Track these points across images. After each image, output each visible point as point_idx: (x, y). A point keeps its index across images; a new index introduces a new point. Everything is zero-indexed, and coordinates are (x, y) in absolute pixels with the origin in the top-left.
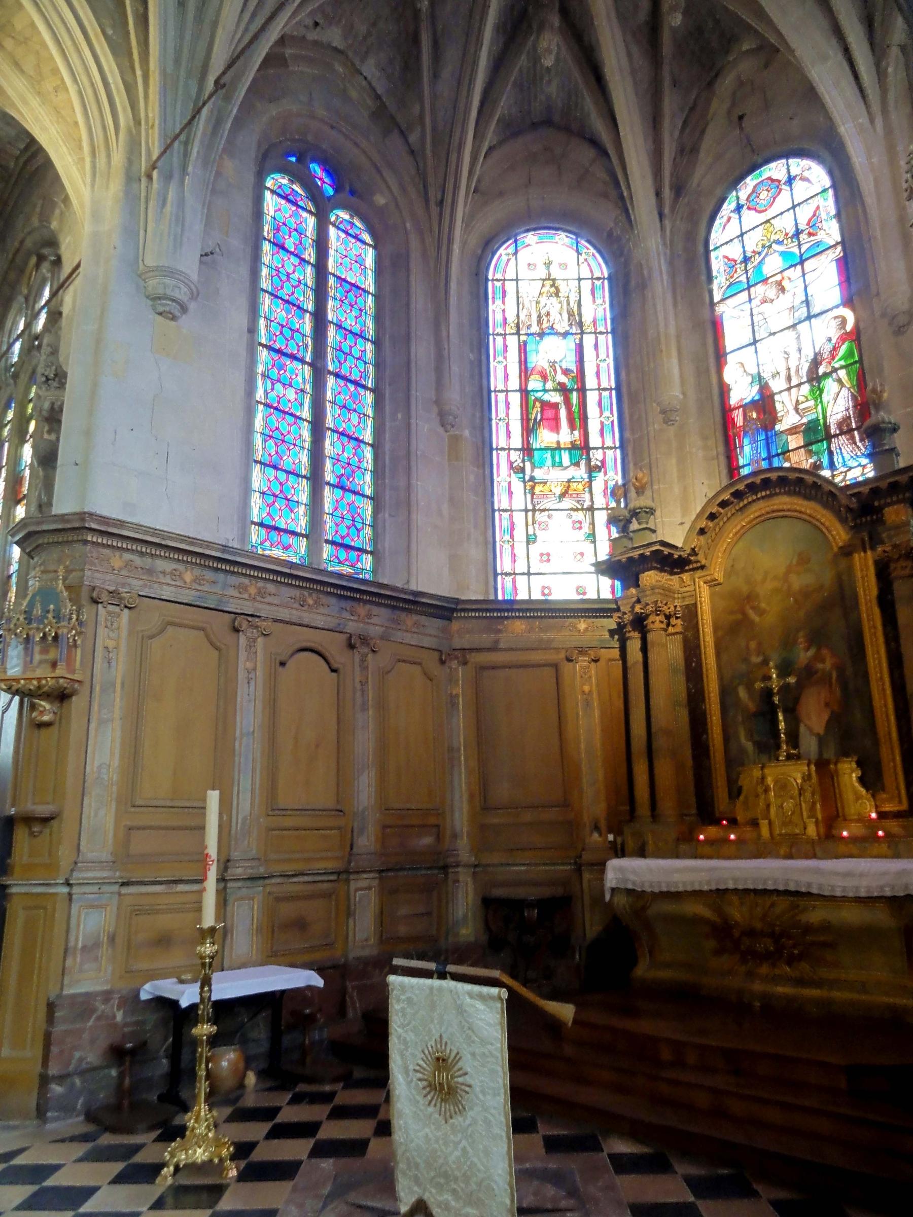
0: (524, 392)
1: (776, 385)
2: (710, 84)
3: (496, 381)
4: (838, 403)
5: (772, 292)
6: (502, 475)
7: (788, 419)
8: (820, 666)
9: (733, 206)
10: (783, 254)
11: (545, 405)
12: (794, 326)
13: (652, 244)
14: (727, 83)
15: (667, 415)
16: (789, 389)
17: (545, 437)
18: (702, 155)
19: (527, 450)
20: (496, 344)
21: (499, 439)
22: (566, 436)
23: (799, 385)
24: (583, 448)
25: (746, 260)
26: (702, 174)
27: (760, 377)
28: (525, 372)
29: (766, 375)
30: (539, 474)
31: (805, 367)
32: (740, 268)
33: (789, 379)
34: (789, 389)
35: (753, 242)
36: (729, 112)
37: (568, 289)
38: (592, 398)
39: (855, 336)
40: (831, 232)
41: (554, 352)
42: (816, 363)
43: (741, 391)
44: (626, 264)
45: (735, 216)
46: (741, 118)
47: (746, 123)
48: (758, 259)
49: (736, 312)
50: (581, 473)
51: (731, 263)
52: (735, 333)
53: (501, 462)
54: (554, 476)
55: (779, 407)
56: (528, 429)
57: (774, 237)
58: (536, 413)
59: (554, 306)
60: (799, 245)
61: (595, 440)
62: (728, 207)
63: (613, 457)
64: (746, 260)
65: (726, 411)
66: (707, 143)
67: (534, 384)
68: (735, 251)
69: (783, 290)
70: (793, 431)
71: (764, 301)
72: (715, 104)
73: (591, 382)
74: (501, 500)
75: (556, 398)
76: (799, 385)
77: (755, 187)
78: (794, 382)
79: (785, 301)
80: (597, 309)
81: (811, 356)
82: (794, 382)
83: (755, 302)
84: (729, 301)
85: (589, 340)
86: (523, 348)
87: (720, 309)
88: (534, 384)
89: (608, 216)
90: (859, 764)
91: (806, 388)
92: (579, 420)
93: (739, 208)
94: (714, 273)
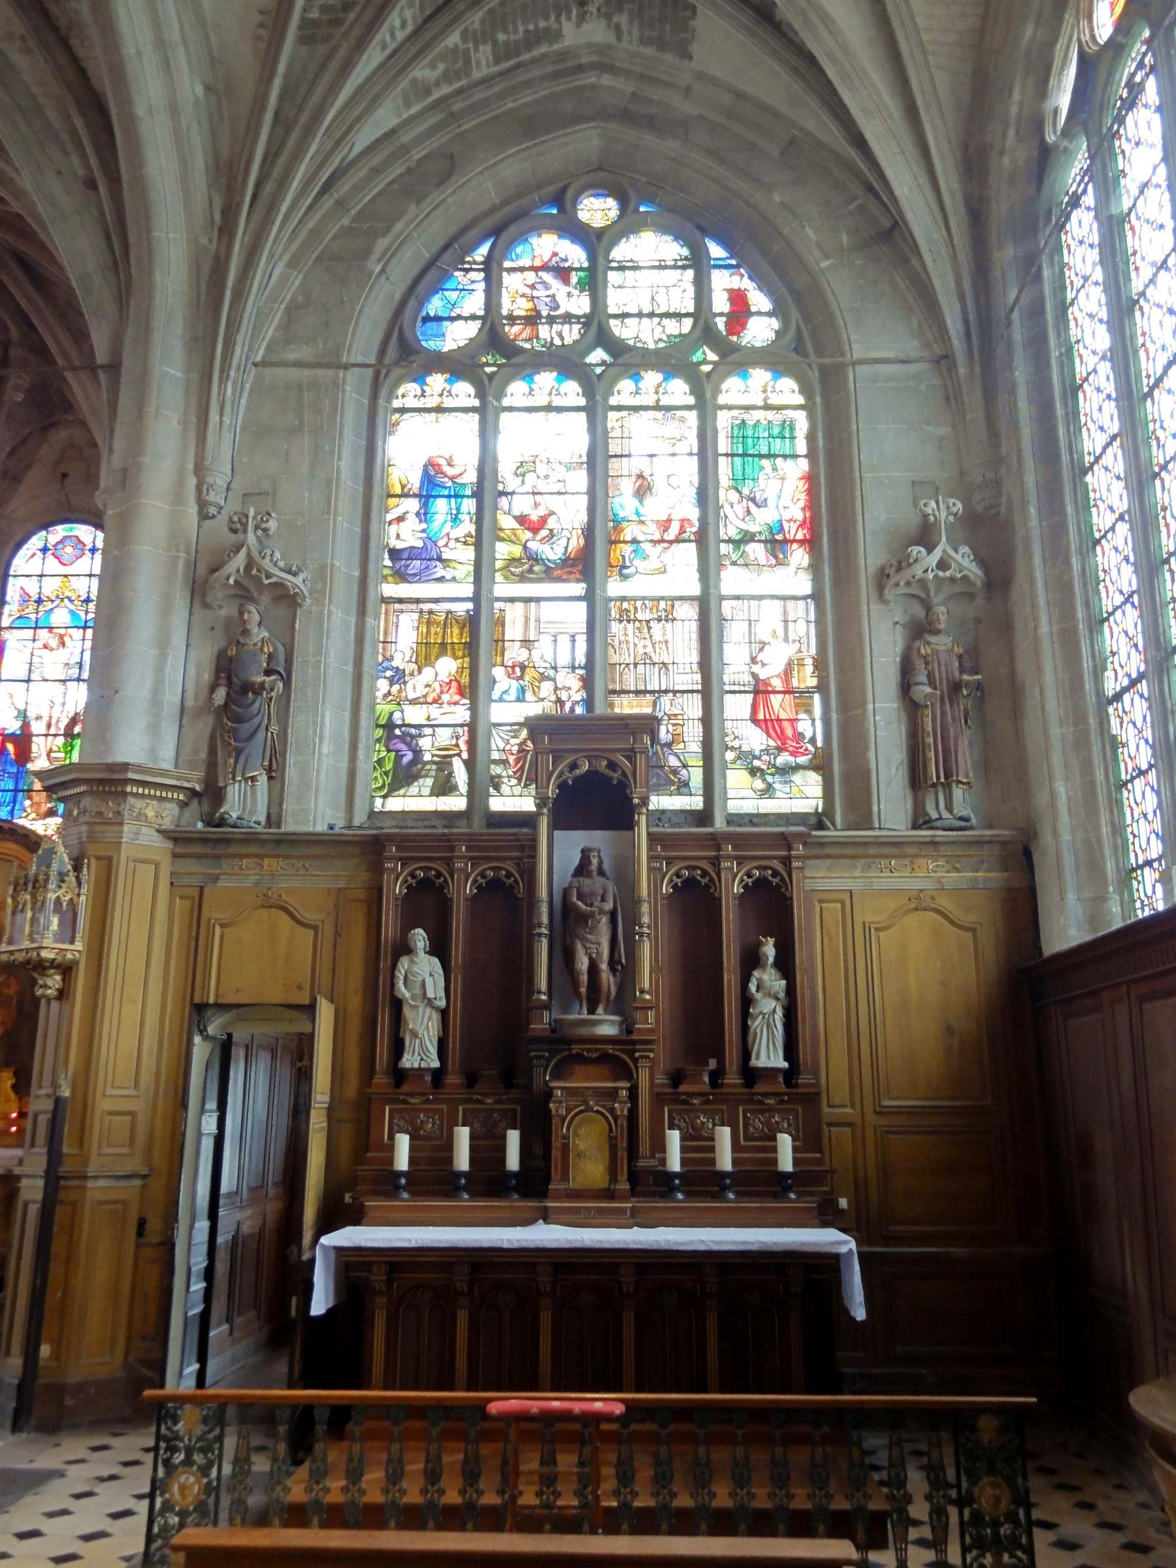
1: (37, 728)
2: (45, 429)
5: (54, 643)
7: (40, 763)
8: (6, 991)
9: (41, 545)
10: (71, 612)
12: (64, 681)
16: (46, 735)
18: (22, 488)
23: (55, 735)
25: (39, 601)
27: (25, 716)
29: (31, 714)
31: (64, 722)
32: (32, 607)
33: (49, 726)
34: (46, 735)
35: (50, 587)
36: (57, 463)
42: (74, 721)
45: (40, 554)
46: (64, 475)
47: (67, 481)
48: (49, 605)
49: (19, 645)
51: (25, 598)
55: (34, 748)
57: (67, 593)
60: (87, 612)
62: (36, 542)
64: (39, 601)
66: (31, 477)
68: (32, 588)
69: (63, 644)
70: (39, 774)
71: (45, 647)
72: (45, 449)
76: (55, 735)
77: (65, 538)
78: (52, 731)
79: (62, 655)
81: (71, 715)
82: (52, 731)
83: (39, 644)
84: (15, 632)
87: (6, 635)
90: (16, 1074)
91: (60, 740)
93: (45, 550)
94: (8, 598)
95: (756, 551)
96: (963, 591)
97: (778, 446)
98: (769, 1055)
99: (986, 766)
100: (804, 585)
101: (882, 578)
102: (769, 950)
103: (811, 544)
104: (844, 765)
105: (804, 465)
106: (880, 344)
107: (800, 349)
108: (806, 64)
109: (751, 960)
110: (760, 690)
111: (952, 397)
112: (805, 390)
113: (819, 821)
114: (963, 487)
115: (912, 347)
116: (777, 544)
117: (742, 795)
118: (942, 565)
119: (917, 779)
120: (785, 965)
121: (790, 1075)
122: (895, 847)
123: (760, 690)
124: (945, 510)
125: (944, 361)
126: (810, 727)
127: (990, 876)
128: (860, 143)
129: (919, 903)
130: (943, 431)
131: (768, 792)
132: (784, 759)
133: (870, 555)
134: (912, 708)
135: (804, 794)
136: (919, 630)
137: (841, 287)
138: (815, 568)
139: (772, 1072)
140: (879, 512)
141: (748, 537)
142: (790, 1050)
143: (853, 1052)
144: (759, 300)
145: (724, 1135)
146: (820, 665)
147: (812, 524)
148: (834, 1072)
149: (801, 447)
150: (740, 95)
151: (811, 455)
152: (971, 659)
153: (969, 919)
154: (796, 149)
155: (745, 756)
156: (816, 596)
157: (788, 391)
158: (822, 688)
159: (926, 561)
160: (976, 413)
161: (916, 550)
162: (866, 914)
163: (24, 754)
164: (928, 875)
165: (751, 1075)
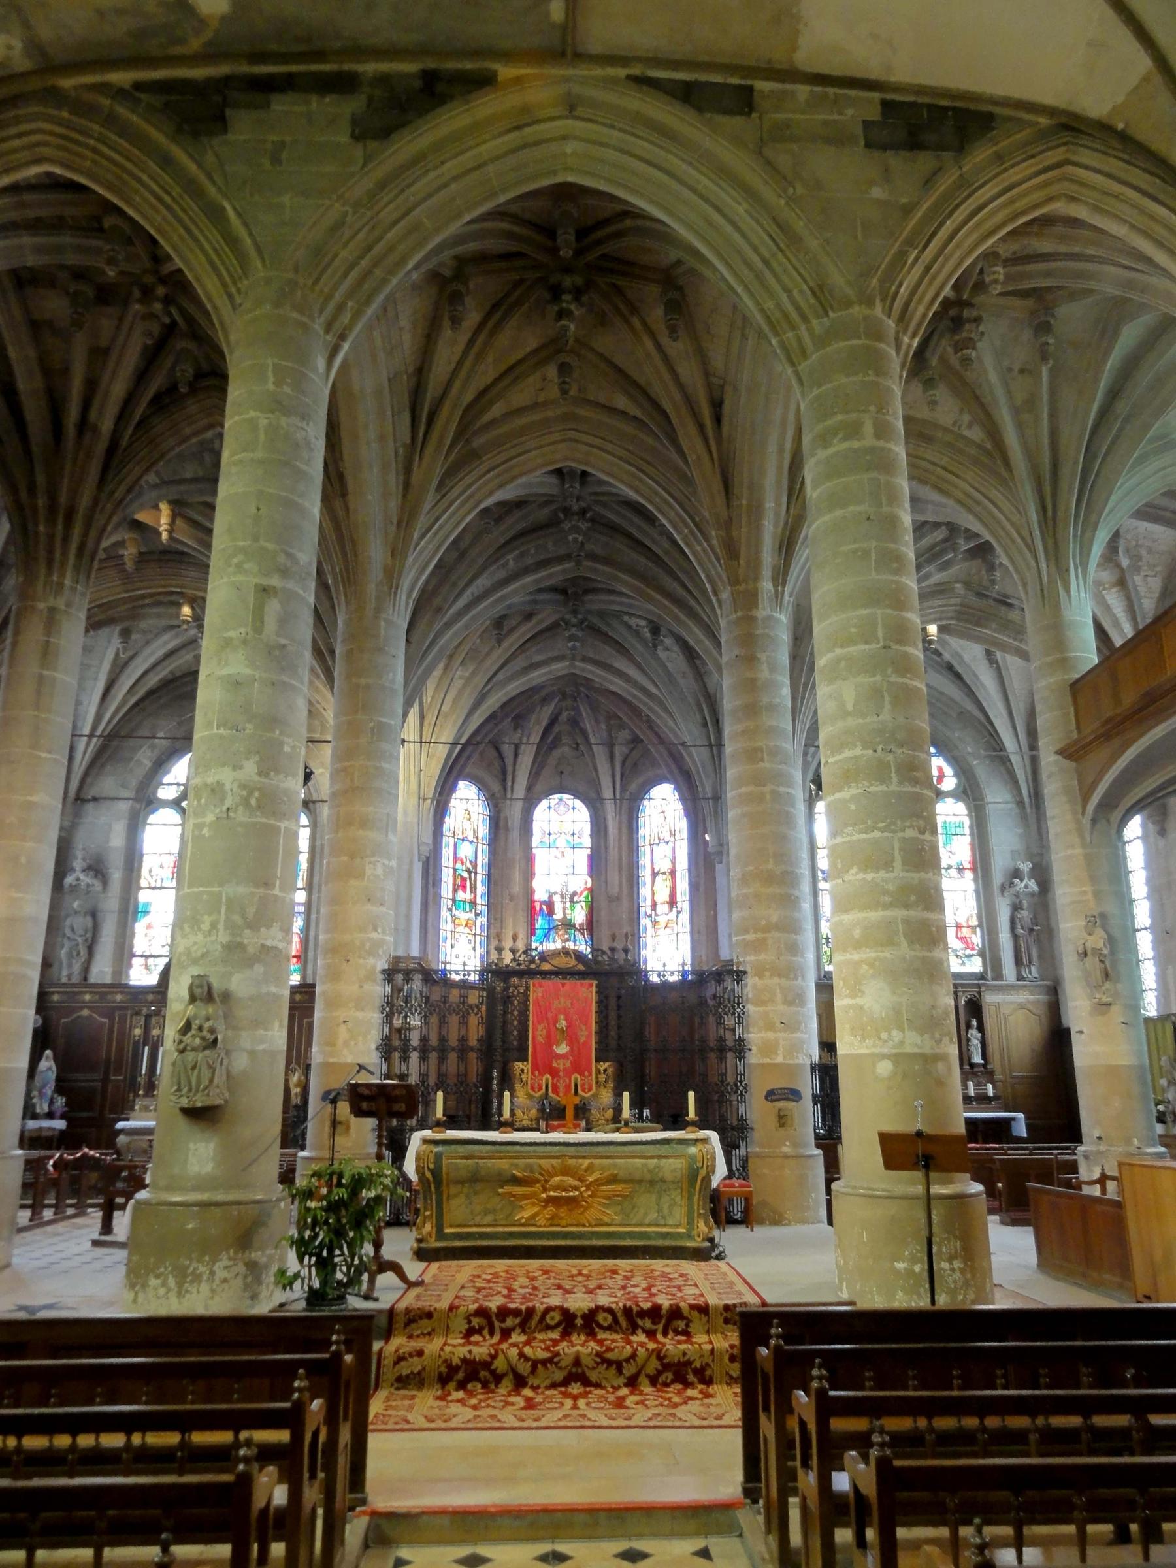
0: (455, 870)
3: (444, 863)
4: (579, 916)
6: (444, 913)
7: (558, 916)
11: (463, 880)
13: (515, 811)
14: (556, 753)
15: (512, 898)
17: (461, 895)
19: (454, 900)
20: (445, 840)
21: (444, 893)
22: (468, 896)
24: (473, 903)
26: (539, 787)
28: (456, 859)
30: (457, 913)
37: (474, 817)
38: (479, 877)
39: (591, 890)
40: (587, 841)
41: (466, 850)
43: (540, 895)
44: (499, 812)
50: (472, 916)
52: (540, 866)
53: (445, 903)
54: (463, 916)
56: (455, 891)
58: (458, 882)
59: (467, 825)
61: (478, 900)
62: (544, 803)
63: (485, 908)
65: (533, 902)
67: (458, 866)
73: (479, 870)
74: (443, 926)
75: (465, 875)
80: (483, 831)
85: (480, 847)
86: (455, 845)
88: (458, 866)
89: (496, 787)
92: (473, 889)
95: (953, 872)
96: (1032, 895)
97: (958, 831)
98: (977, 1059)
99: (1040, 957)
100: (971, 886)
101: (1003, 889)
102: (974, 1023)
103: (974, 869)
104: (990, 952)
105: (968, 839)
106: (997, 797)
107: (965, 792)
108: (970, 693)
109: (969, 1026)
110: (959, 927)
111: (1024, 817)
112: (968, 808)
113: (982, 976)
114: (1030, 857)
115: (1008, 797)
116: (961, 870)
117: (955, 966)
118: (1026, 886)
119: (1018, 961)
120: (981, 1028)
121: (984, 1066)
122: (1012, 987)
123: (959, 927)
124: (1025, 867)
125: (1020, 803)
126: (977, 940)
127: (1043, 998)
128: (992, 724)
129: (1021, 1006)
130: (1020, 831)
131: (963, 964)
132: (968, 952)
133: (998, 878)
134: (1015, 937)
135: (975, 966)
136: (1016, 908)
137: (982, 770)
138: (975, 880)
139: (978, 1065)
140: (1000, 863)
141: (950, 867)
142: (984, 1055)
143: (1002, 1058)
144: (948, 771)
145: (971, 1084)
146: (979, 917)
147: (973, 862)
148: (995, 1064)
149: (967, 831)
150: (942, 693)
151: (972, 834)
152: (1035, 921)
153: (1038, 1012)
154: (963, 715)
155: (955, 951)
156: (977, 891)
157: (961, 808)
158: (980, 925)
159: (1020, 885)
160: (1034, 827)
161: (1017, 881)
162: (1005, 1010)
163: (551, 912)
164: (1023, 997)
165: (972, 1066)
